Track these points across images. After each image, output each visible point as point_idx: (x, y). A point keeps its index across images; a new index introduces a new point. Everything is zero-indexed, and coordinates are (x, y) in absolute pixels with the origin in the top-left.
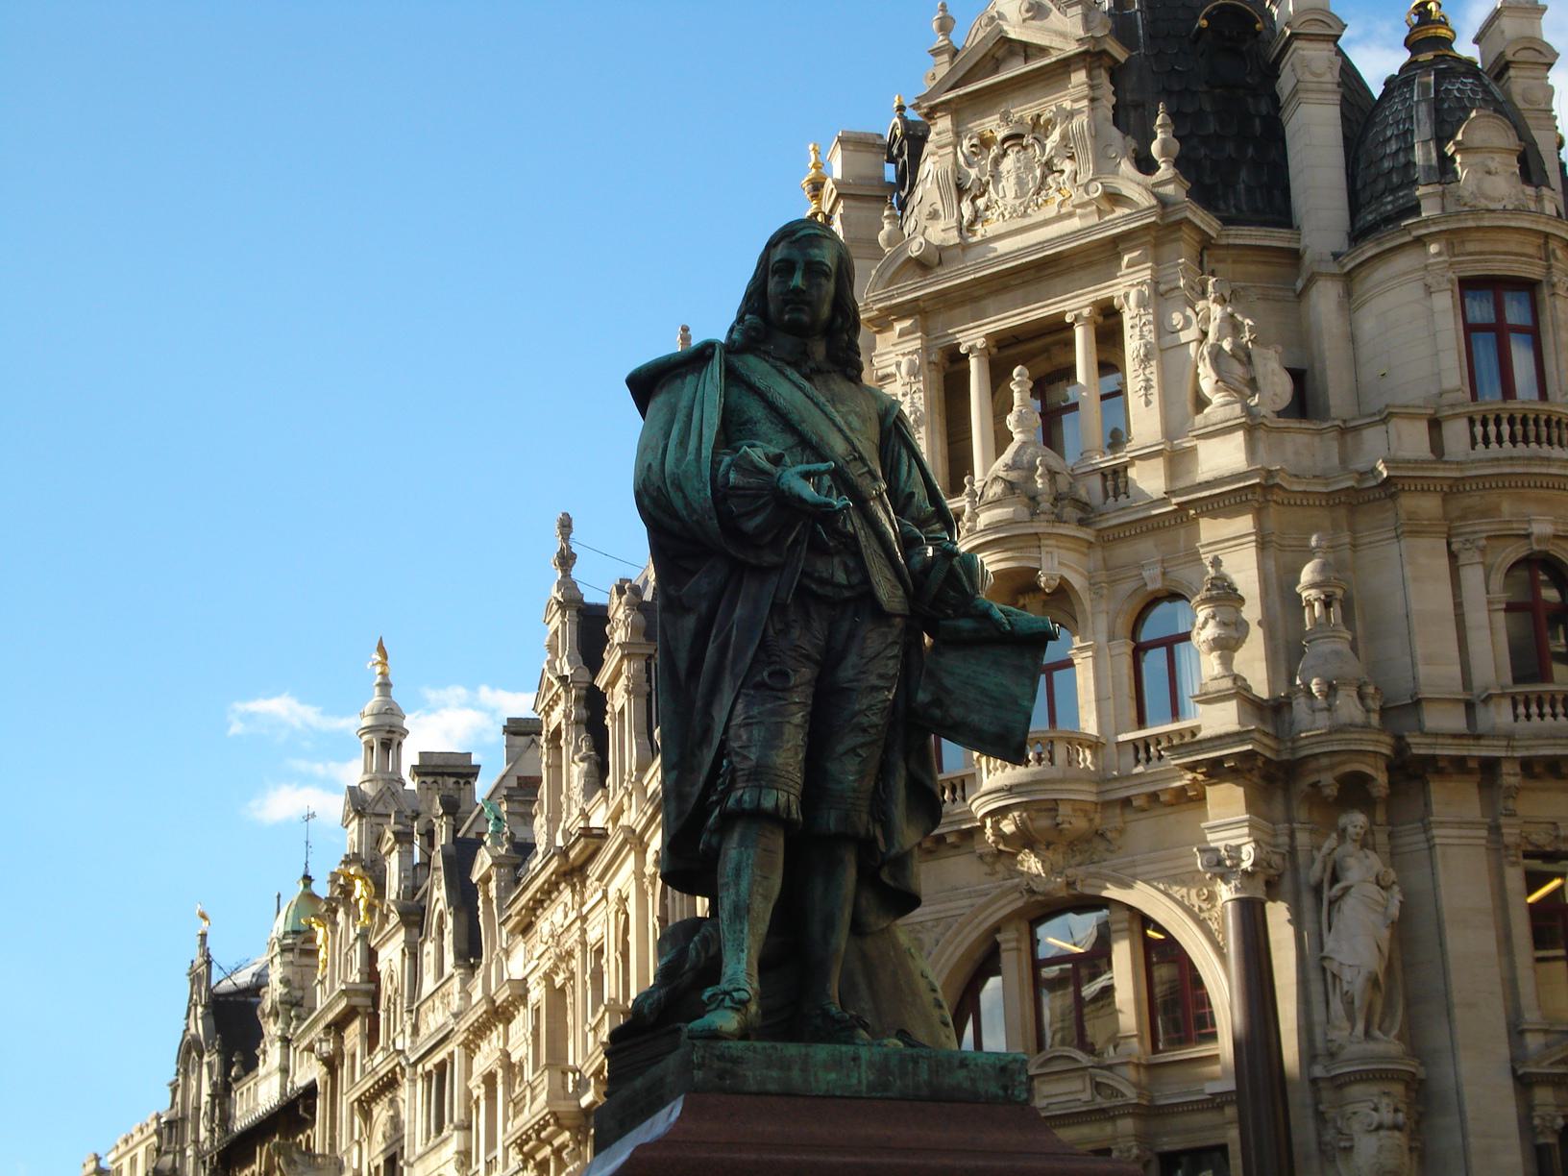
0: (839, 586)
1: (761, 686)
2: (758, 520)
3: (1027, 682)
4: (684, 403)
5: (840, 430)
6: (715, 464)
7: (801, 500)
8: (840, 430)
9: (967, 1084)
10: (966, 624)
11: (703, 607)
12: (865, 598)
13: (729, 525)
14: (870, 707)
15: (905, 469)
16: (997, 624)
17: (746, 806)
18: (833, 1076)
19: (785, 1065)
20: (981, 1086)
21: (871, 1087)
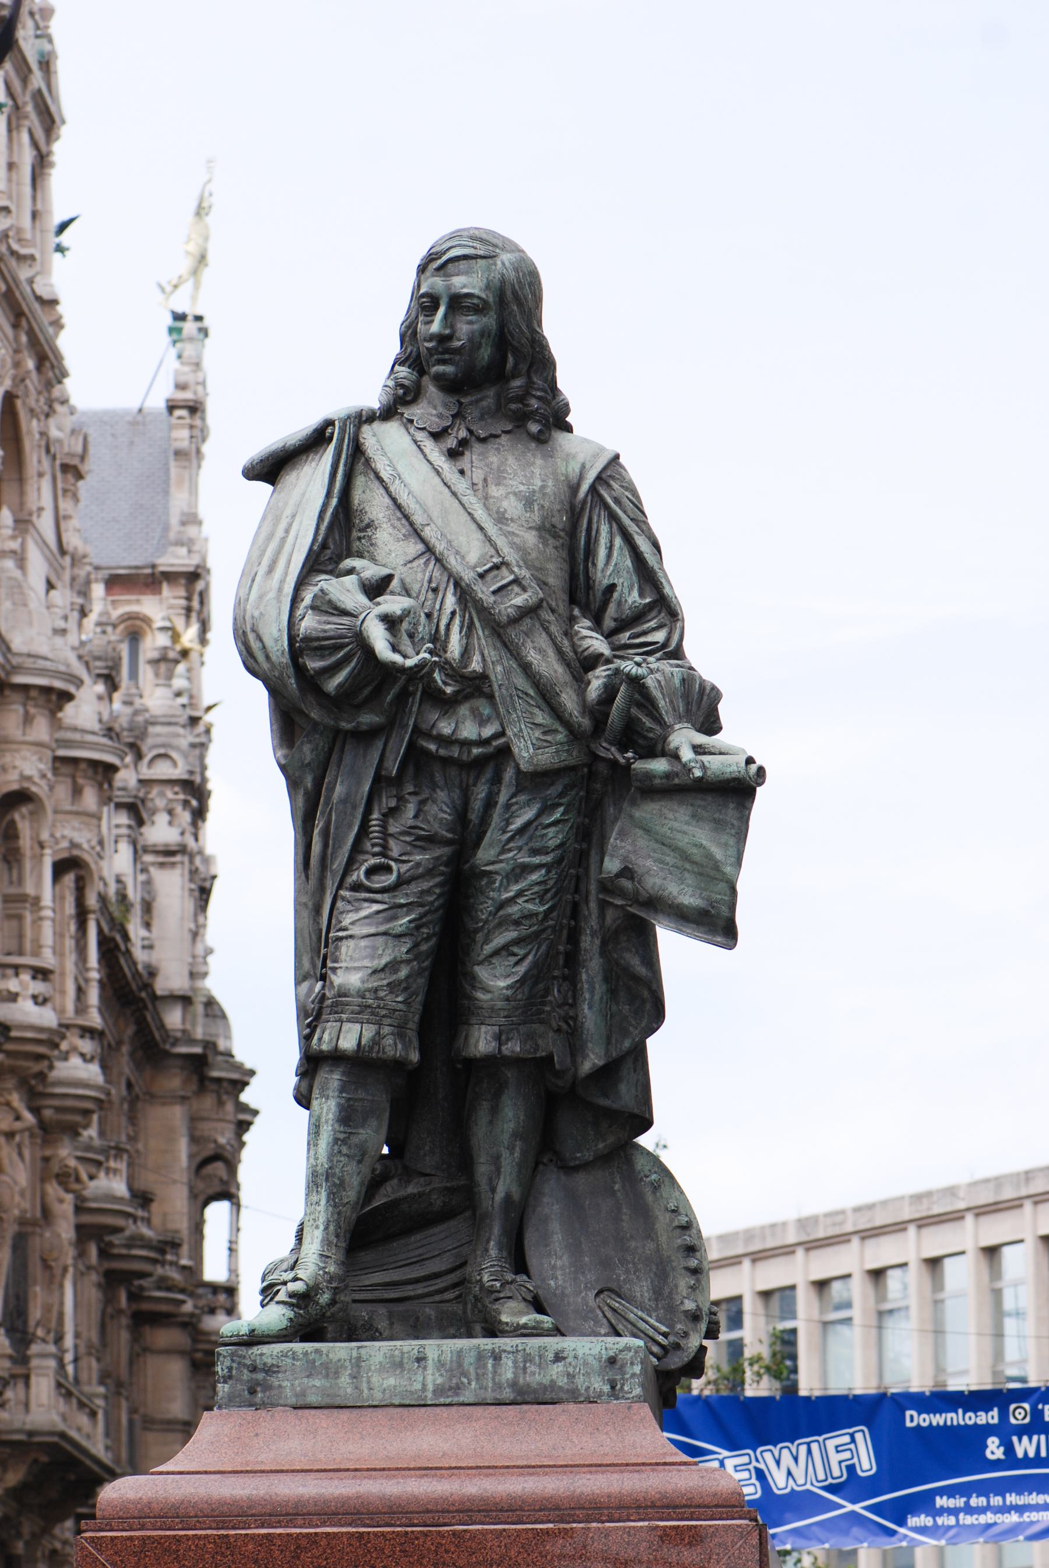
0: (467, 744)
1: (357, 887)
3: (732, 841)
4: (288, 512)
5: (481, 529)
9: (563, 1381)
10: (659, 766)
14: (520, 894)
15: (602, 553)
19: (331, 1371)
20: (580, 1382)
21: (439, 1391)
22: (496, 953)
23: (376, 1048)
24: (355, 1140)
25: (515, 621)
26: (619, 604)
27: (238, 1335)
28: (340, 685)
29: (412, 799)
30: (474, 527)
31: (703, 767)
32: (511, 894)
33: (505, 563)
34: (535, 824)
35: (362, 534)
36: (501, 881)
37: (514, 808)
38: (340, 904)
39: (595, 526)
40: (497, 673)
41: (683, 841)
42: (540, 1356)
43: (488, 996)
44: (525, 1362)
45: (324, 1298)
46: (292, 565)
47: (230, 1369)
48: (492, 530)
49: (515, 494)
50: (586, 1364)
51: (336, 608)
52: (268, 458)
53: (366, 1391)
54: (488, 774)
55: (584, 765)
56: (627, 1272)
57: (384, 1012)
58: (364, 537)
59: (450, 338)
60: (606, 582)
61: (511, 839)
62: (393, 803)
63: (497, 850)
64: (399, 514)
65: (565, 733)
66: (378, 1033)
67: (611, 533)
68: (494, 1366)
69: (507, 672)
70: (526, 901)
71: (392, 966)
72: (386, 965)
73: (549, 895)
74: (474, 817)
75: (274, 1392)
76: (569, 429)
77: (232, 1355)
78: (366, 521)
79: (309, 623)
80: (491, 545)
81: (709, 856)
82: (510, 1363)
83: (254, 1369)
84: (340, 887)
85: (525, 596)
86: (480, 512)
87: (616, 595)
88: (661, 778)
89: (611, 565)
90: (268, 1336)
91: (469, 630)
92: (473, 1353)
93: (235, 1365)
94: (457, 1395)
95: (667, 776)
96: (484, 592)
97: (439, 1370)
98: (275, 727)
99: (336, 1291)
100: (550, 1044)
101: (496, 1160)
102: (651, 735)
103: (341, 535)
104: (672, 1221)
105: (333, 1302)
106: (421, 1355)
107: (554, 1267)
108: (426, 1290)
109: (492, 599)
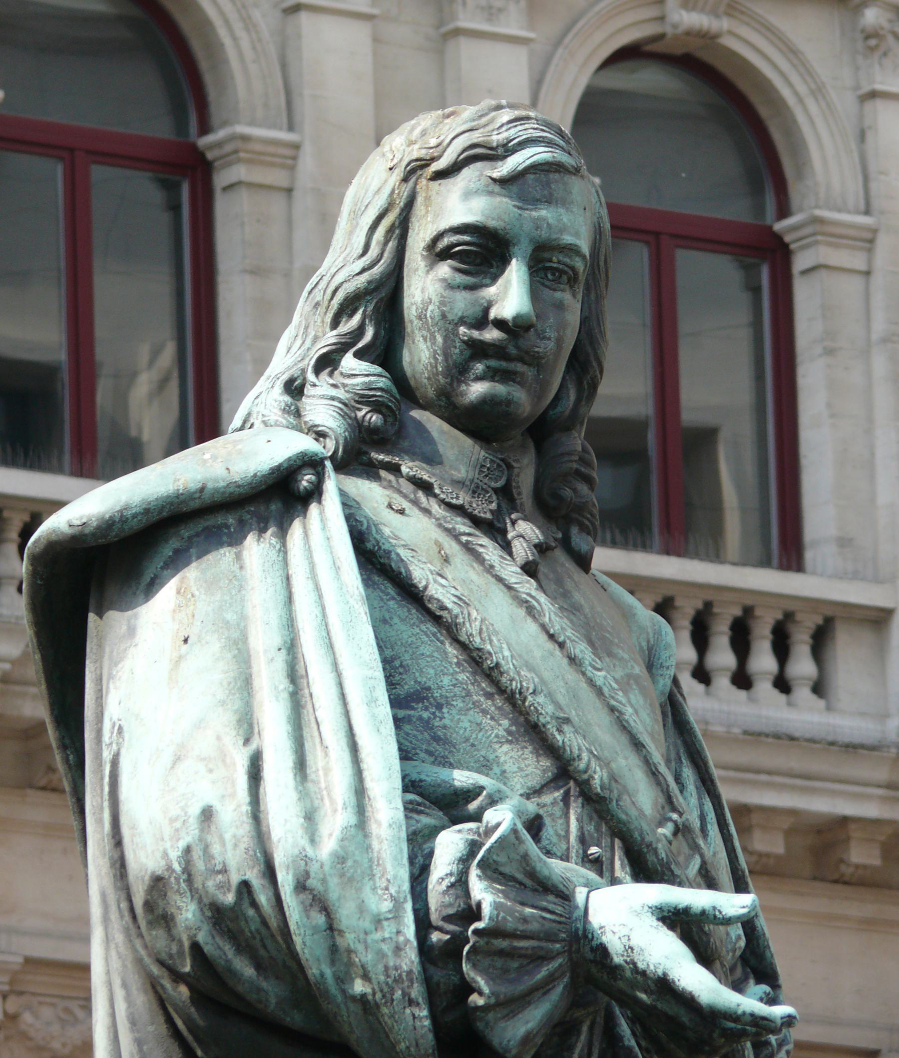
7: (664, 986)
30: (624, 739)
51: (532, 874)
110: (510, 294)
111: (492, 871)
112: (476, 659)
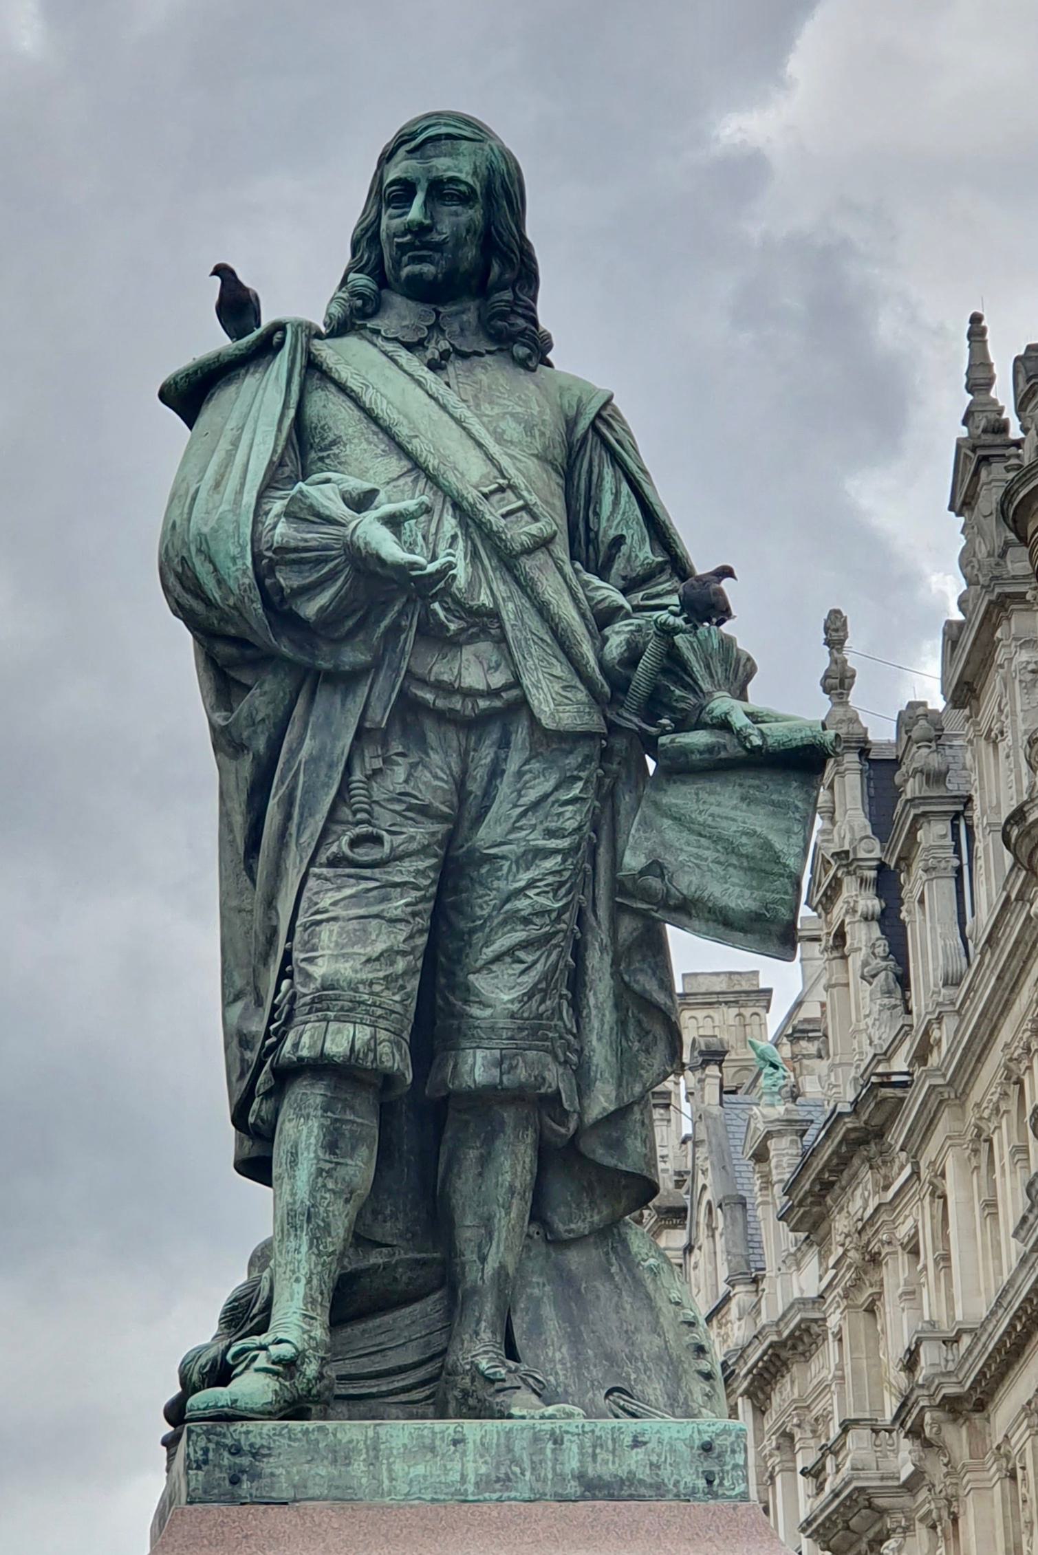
1: (334, 862)
2: (323, 599)
5: (480, 445)
6: (259, 513)
8: (480, 445)
9: (643, 1474)
10: (699, 738)
11: (261, 744)
12: (518, 706)
13: (278, 607)
14: (531, 884)
15: (607, 499)
16: (741, 736)
17: (305, 1053)
18: (420, 1469)
21: (484, 1483)
22: (498, 958)
23: (371, 1055)
24: (341, 1171)
25: (528, 552)
26: (629, 559)
27: (215, 1406)
28: (322, 609)
29: (400, 760)
30: (470, 443)
31: (762, 735)
32: (522, 884)
33: (512, 487)
34: (552, 799)
35: (325, 454)
36: (510, 867)
37: (527, 777)
38: (312, 883)
39: (596, 470)
40: (508, 612)
41: (730, 829)
42: (613, 1440)
43: (488, 1012)
44: (594, 1447)
45: (311, 1369)
46: (249, 476)
47: (206, 1451)
48: (494, 449)
49: (512, 415)
50: (673, 1450)
51: (318, 515)
52: (196, 372)
53: (386, 1483)
54: (495, 734)
55: (601, 736)
56: (637, 1370)
57: (379, 1012)
58: (328, 456)
59: (429, 229)
60: (612, 533)
61: (523, 815)
62: (378, 763)
63: (507, 826)
64: (374, 428)
65: (585, 692)
66: (374, 1037)
67: (615, 476)
68: (553, 1450)
69: (519, 614)
70: (538, 894)
71: (389, 955)
72: (381, 954)
73: (563, 891)
74: (475, 787)
75: (265, 1481)
76: (550, 365)
77: (207, 1433)
78: (331, 437)
79: (283, 532)
80: (494, 465)
81: (767, 846)
82: (575, 1448)
83: (237, 1451)
84: (312, 862)
85: (539, 525)
86: (478, 426)
87: (624, 549)
88: (701, 753)
89: (616, 515)
90: (252, 1411)
91: (474, 556)
92: (528, 1434)
93: (212, 1446)
94: (508, 1489)
95: (710, 749)
96: (492, 513)
97: (482, 1456)
98: (208, 685)
99: (324, 1361)
100: (556, 1077)
101: (487, 1223)
102: (683, 705)
103: (303, 446)
104: (676, 1315)
105: (320, 1377)
106: (458, 1436)
107: (552, 1360)
108: (391, 1387)
109: (503, 522)
110: (415, 212)
111: (288, 514)
112: (371, 416)
